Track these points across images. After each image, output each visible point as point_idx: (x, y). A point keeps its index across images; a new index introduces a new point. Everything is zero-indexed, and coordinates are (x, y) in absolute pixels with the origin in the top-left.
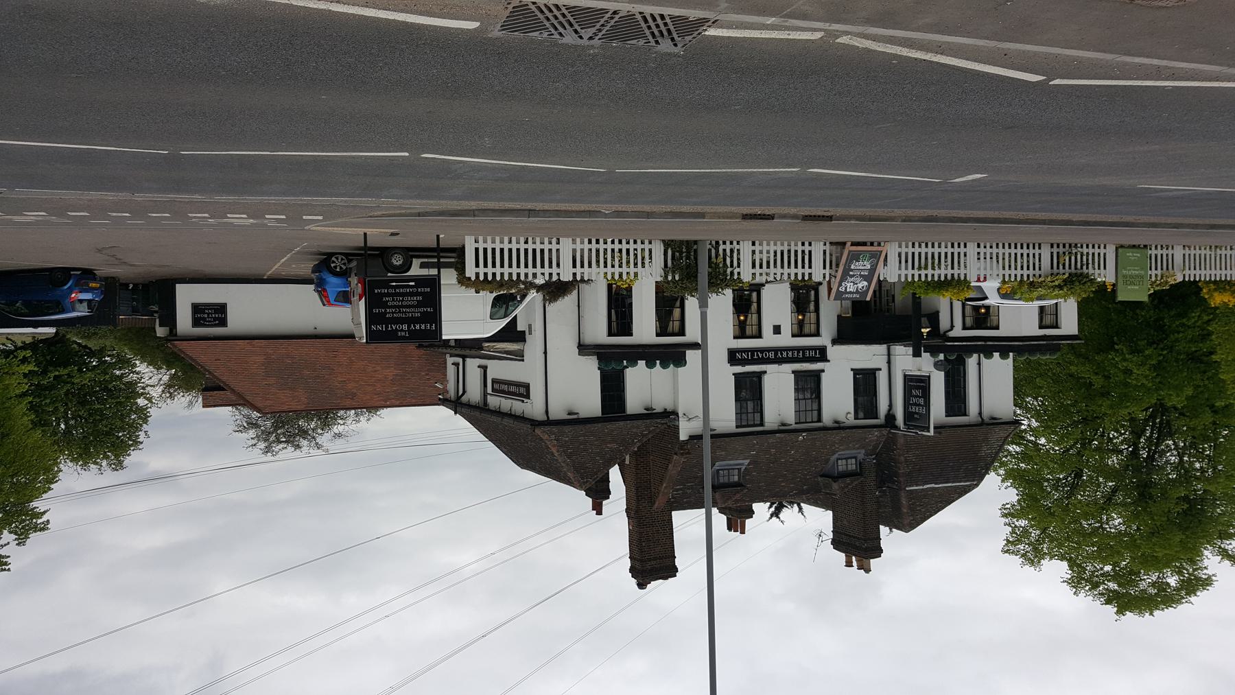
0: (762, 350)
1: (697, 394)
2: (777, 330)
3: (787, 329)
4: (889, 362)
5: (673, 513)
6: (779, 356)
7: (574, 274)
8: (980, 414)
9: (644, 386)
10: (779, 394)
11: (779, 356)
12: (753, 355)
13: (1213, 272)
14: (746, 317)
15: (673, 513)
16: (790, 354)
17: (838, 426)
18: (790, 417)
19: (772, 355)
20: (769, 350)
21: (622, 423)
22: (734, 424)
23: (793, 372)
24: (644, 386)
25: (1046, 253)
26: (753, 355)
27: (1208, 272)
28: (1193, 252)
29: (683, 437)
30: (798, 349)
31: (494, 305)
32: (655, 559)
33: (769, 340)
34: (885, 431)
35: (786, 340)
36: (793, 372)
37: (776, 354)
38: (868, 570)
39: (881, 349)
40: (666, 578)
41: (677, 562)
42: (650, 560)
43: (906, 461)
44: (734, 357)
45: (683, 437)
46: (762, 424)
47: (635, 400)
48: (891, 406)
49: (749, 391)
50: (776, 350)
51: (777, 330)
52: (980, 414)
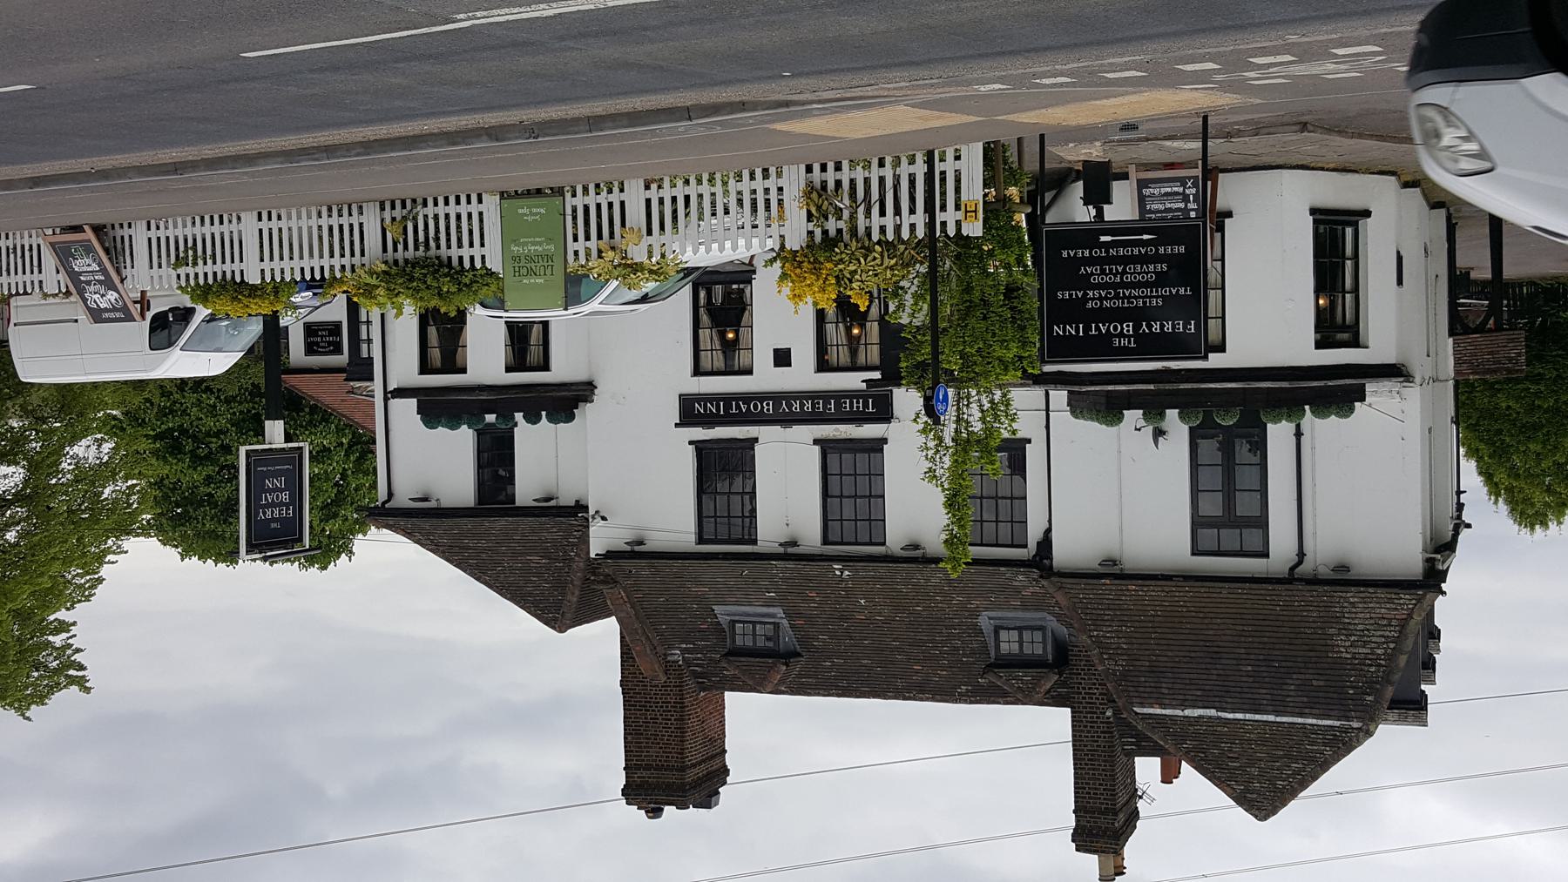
0: (747, 398)
2: (782, 358)
3: (804, 354)
6: (784, 410)
9: (543, 457)
10: (788, 484)
11: (784, 410)
12: (728, 407)
13: (326, 262)
14: (737, 333)
16: (808, 406)
17: (916, 558)
19: (768, 407)
20: (762, 397)
22: (693, 538)
23: (816, 442)
24: (543, 457)
25: (372, 222)
26: (728, 407)
27: (316, 263)
28: (667, 194)
30: (826, 396)
31: (152, 330)
33: (765, 378)
34: (1035, 573)
35: (803, 376)
36: (816, 442)
37: (777, 406)
44: (691, 411)
46: (755, 542)
47: (526, 489)
49: (723, 473)
50: (777, 397)
51: (782, 358)
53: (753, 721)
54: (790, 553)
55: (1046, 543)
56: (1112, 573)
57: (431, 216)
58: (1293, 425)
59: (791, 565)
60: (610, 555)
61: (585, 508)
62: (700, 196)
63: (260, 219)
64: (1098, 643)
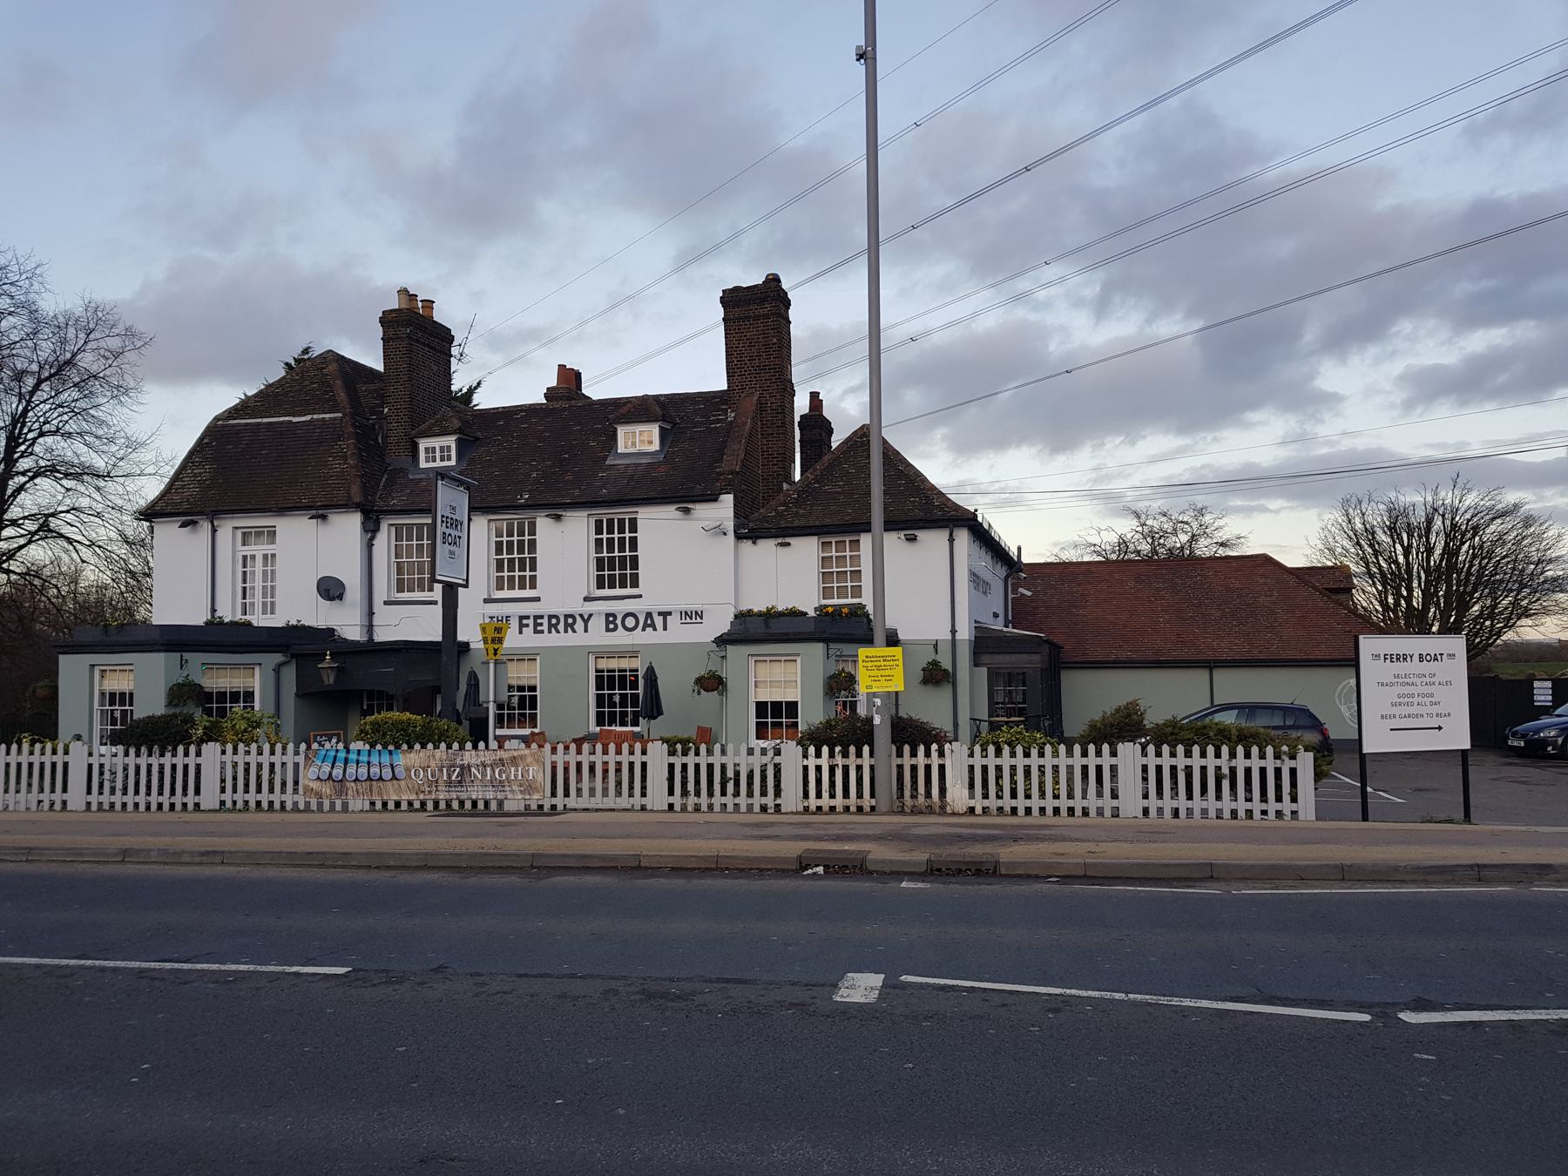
1: (700, 567)
4: (371, 614)
5: (725, 387)
7: (1114, 754)
8: (214, 531)
15: (725, 387)
18: (543, 524)
21: (827, 521)
29: (728, 499)
32: (756, 318)
38: (404, 292)
39: (381, 636)
40: (737, 289)
41: (720, 312)
42: (766, 316)
43: (345, 458)
45: (728, 499)
48: (370, 546)
52: (214, 531)
53: (702, 368)
54: (556, 508)
55: (371, 529)
56: (320, 510)
57: (119, 793)
58: (218, 614)
59: (559, 500)
60: (713, 498)
61: (739, 537)
62: (1028, 797)
63: (64, 803)
64: (345, 458)
